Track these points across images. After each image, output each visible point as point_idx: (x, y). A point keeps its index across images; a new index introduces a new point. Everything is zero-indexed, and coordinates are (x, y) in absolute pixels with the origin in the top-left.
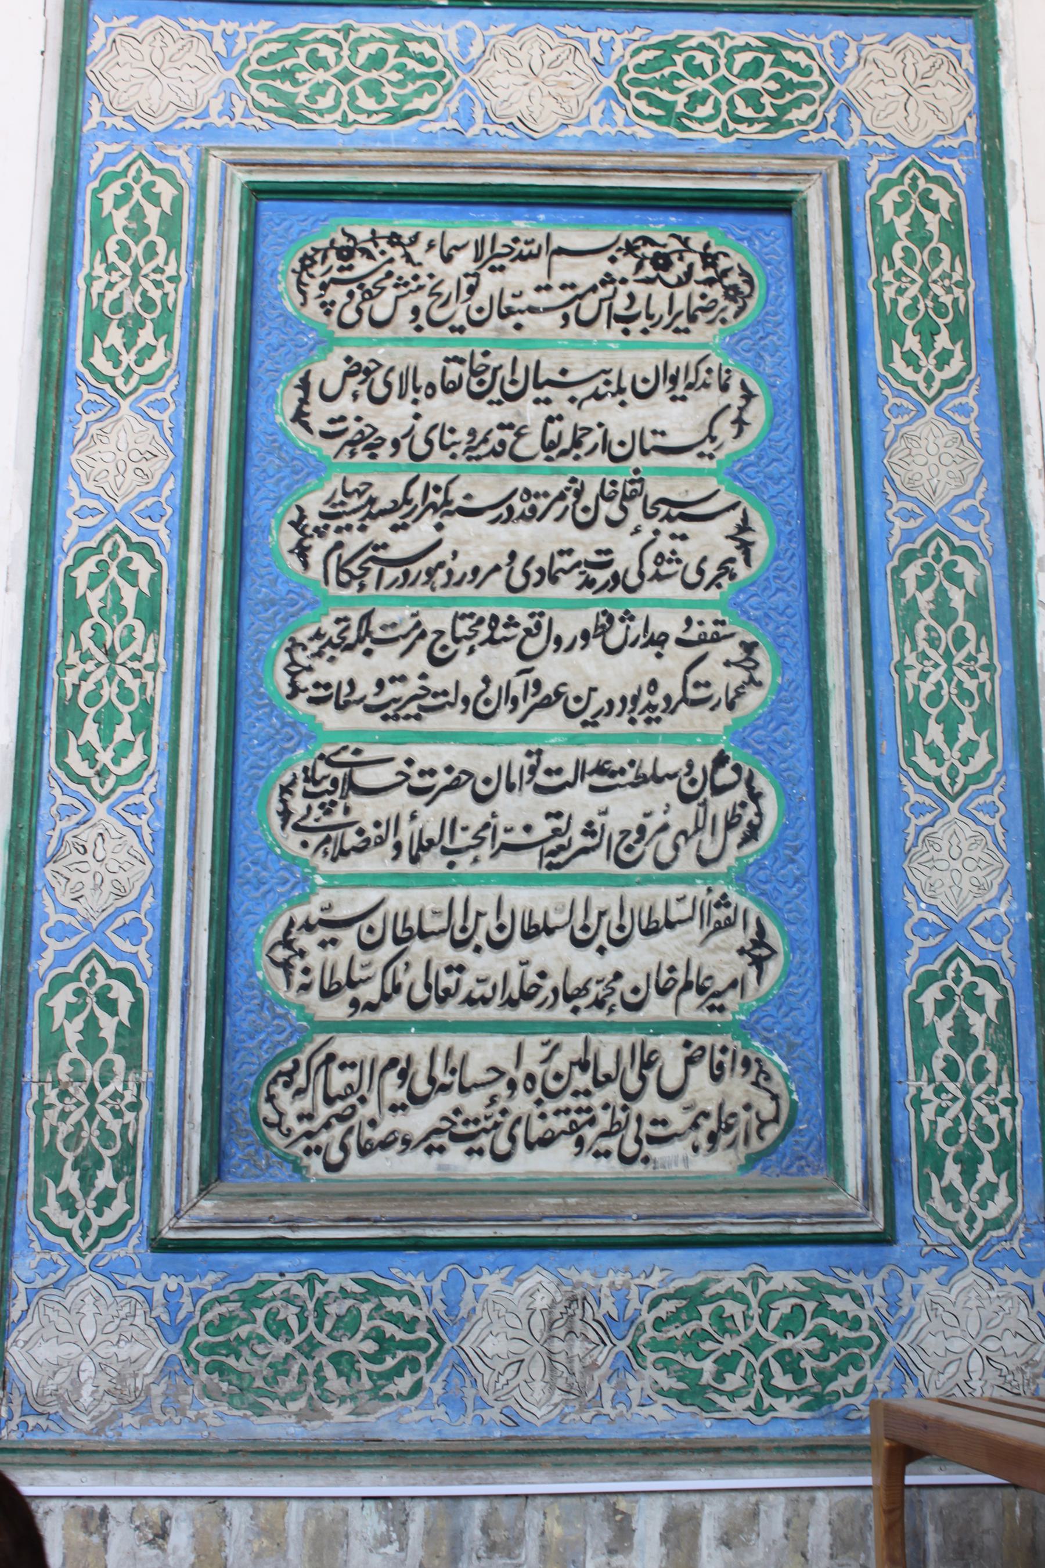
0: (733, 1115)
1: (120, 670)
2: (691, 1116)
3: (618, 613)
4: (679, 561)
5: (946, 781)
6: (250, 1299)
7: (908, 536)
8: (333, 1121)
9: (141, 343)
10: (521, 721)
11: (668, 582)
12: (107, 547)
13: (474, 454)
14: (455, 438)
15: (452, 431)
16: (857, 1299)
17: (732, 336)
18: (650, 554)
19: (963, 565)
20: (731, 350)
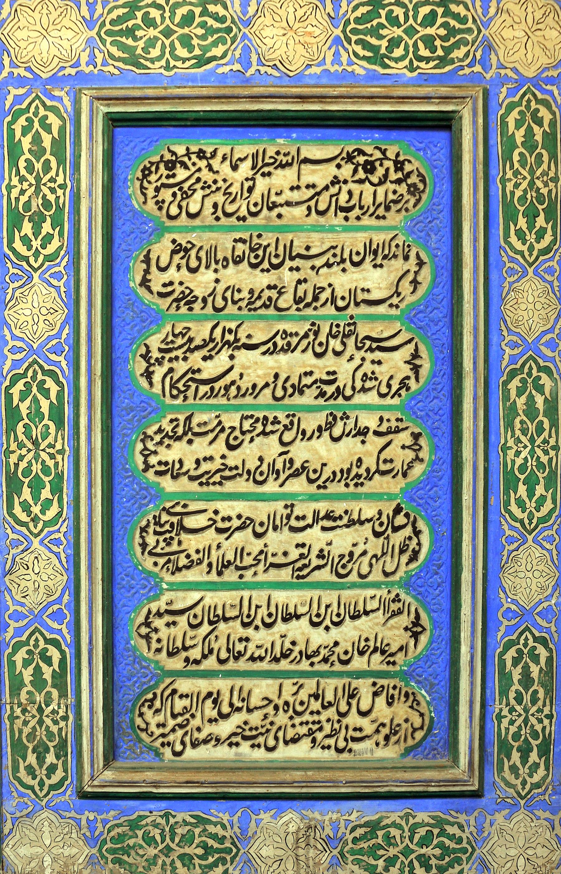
0: (399, 725)
1: (42, 453)
2: (375, 725)
3: (339, 415)
4: (376, 379)
5: (526, 521)
6: (134, 825)
7: (513, 359)
8: (177, 727)
9: (44, 232)
10: (281, 485)
11: (370, 393)
12: (30, 373)
13: (253, 307)
14: (241, 296)
15: (239, 291)
16: (461, 827)
17: (412, 220)
18: (359, 374)
19: (545, 380)
20: (410, 231)
